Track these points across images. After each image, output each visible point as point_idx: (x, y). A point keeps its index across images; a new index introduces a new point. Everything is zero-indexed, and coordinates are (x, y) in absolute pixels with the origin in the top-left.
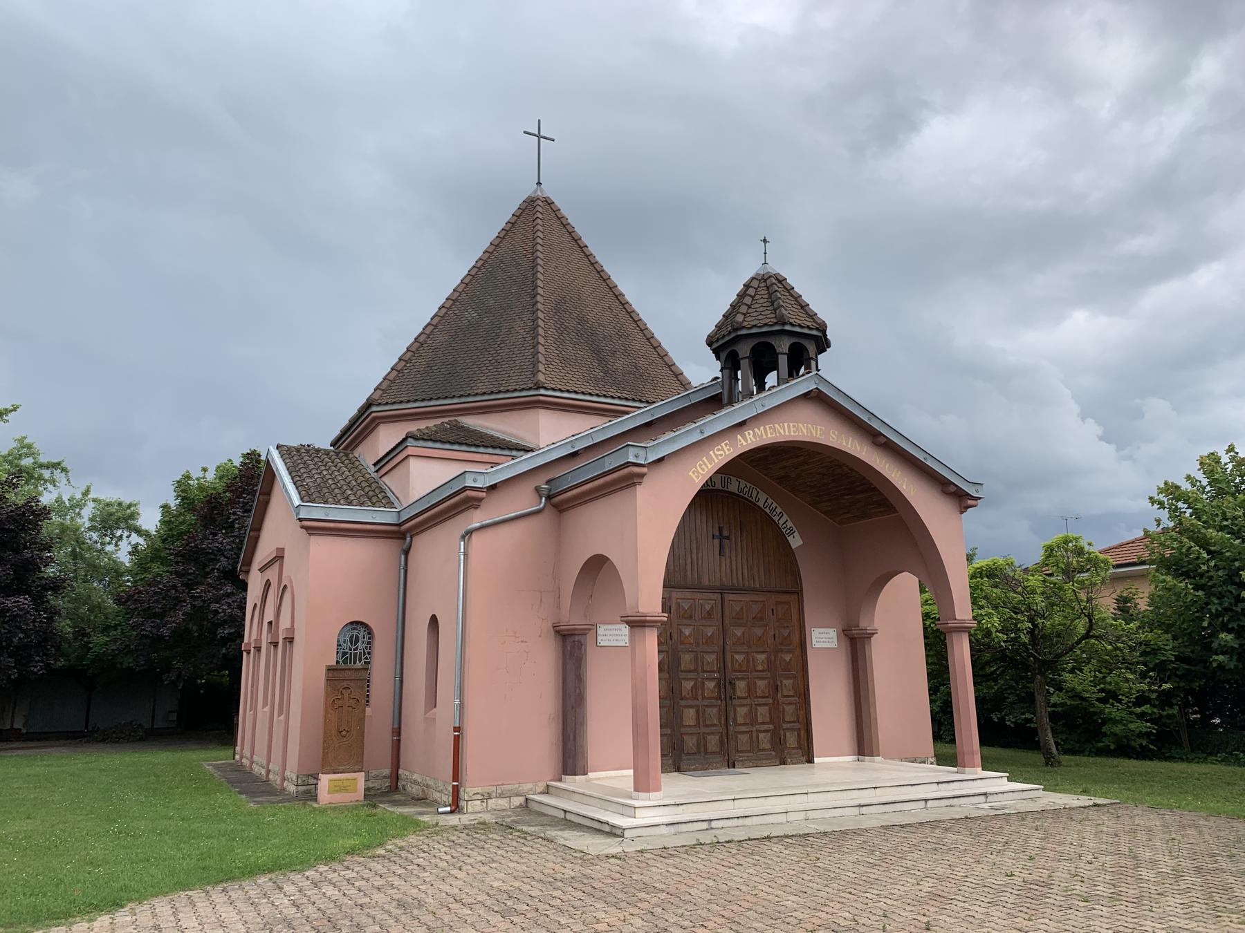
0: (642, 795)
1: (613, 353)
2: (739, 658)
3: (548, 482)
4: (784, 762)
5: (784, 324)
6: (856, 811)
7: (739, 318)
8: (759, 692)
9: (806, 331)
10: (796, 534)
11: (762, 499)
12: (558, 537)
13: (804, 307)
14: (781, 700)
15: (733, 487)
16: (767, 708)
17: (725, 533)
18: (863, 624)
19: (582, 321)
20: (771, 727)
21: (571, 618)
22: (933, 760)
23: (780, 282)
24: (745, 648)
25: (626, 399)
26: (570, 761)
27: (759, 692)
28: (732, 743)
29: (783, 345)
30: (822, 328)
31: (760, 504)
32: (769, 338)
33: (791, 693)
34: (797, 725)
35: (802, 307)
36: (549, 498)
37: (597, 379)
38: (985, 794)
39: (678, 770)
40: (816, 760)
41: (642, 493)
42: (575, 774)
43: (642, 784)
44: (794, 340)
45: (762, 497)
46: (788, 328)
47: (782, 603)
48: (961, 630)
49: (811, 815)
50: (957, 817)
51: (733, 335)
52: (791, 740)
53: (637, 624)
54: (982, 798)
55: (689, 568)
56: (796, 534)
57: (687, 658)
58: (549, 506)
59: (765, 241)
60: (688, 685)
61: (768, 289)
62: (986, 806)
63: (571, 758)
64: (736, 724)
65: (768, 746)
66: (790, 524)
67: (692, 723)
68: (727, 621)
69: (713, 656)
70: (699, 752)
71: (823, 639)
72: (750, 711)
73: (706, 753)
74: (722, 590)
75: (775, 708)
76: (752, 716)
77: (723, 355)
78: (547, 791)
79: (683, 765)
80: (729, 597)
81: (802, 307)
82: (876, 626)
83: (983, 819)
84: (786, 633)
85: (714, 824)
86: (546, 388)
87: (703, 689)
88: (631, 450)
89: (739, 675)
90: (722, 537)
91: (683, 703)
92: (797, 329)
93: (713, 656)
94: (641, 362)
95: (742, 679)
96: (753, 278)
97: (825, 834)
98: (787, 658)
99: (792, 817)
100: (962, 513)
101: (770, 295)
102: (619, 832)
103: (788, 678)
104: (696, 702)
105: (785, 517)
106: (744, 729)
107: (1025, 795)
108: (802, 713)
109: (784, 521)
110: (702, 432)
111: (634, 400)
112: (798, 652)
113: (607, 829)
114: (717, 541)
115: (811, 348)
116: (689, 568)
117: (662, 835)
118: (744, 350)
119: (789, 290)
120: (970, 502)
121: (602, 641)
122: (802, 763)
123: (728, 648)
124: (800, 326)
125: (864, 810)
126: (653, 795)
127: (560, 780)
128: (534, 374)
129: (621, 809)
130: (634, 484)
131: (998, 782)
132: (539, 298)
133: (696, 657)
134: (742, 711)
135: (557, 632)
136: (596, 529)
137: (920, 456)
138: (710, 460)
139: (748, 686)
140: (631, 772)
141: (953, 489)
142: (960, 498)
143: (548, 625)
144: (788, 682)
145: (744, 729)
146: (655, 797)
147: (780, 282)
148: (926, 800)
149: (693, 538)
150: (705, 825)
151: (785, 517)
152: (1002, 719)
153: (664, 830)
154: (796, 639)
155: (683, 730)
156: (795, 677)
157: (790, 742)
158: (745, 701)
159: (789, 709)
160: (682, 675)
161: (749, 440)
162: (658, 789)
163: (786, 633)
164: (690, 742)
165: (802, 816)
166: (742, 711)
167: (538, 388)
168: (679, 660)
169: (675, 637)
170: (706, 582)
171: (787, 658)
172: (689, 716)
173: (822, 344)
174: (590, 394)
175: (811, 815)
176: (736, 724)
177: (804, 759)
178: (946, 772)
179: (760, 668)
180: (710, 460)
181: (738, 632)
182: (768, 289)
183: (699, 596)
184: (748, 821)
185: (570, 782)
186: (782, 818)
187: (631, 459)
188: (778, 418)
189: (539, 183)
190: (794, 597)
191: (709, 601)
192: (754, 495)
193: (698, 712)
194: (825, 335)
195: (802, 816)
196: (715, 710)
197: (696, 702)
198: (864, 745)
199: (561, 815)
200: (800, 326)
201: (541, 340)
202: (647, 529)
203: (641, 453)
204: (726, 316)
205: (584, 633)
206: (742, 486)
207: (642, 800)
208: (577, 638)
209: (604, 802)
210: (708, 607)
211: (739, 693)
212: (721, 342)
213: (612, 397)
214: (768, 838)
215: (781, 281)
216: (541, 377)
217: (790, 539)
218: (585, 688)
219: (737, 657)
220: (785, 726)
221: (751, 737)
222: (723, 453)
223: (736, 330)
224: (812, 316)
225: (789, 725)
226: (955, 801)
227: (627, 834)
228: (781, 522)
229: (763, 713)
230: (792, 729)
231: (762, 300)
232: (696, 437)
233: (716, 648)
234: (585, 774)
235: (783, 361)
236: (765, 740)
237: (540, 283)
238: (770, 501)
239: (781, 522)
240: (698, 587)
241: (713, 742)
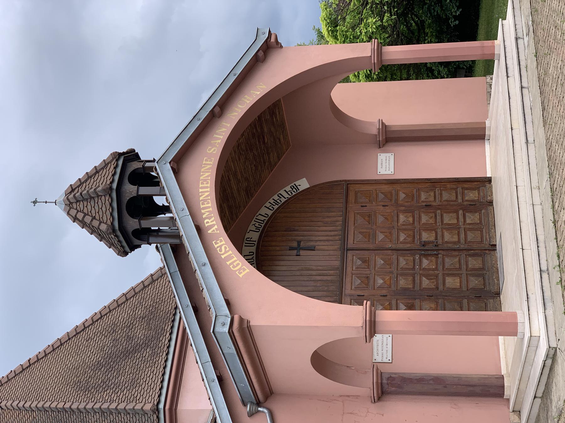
0: (520, 330)
1: (129, 338)
2: (402, 237)
3: (245, 405)
4: (491, 203)
5: (111, 188)
6: (531, 146)
7: (103, 227)
8: (432, 221)
9: (119, 170)
10: (297, 183)
11: (266, 211)
12: (296, 396)
13: (97, 171)
14: (438, 203)
15: (255, 236)
16: (445, 215)
17: (295, 244)
18: (374, 131)
19: (98, 366)
20: (461, 212)
21: (366, 386)
22: (488, 78)
23: (73, 190)
24: (395, 232)
25: (172, 327)
26: (492, 391)
27: (432, 221)
28: (475, 246)
29: (130, 190)
30: (117, 156)
31: (270, 213)
32: (125, 203)
33: (432, 194)
34: (460, 190)
35: (97, 172)
36: (259, 404)
37: (153, 354)
38: (517, 39)
39: (498, 294)
40: (489, 175)
41: (257, 320)
42: (503, 387)
43: (510, 328)
44: (126, 181)
45: (264, 211)
46: (115, 186)
47: (356, 197)
48: (380, 53)
49: (535, 184)
50: (535, 63)
51: (119, 233)
52: (472, 195)
53: (372, 328)
54: (520, 41)
55: (325, 278)
56: (297, 183)
57: (402, 283)
58: (265, 404)
59: (35, 202)
60: (426, 282)
61: (78, 202)
62: (526, 39)
63: (490, 389)
64: (459, 241)
65: (477, 215)
66: (288, 188)
67: (458, 280)
68: (371, 246)
69: (401, 259)
70: (483, 276)
71: (386, 165)
72: (448, 229)
73: (483, 269)
74: (345, 250)
75: (446, 208)
76: (451, 228)
77: (136, 242)
78: (518, 412)
79: (494, 289)
80: (351, 243)
81: (97, 172)
82: (376, 121)
83: (536, 43)
84: (381, 196)
85: (544, 268)
86: (158, 403)
87: (430, 269)
88: (217, 329)
89: (417, 237)
90: (299, 248)
91: (441, 288)
92: (117, 178)
93: (401, 259)
94: (139, 312)
95: (420, 235)
96: (68, 214)
97: (551, 174)
98: (402, 196)
99: (537, 200)
100: (281, 47)
101: (84, 200)
102: (552, 352)
103: (419, 196)
104: (440, 277)
105: (282, 192)
106: (462, 236)
107: (517, 6)
108: (448, 186)
109: (285, 193)
110: (204, 265)
111: (173, 321)
112: (397, 187)
113: (549, 362)
114: (302, 252)
115: (135, 165)
116: (325, 278)
117: (554, 313)
118: (133, 224)
119: (81, 183)
120: (273, 40)
121: (387, 358)
122: (491, 187)
123: (394, 246)
124: (114, 175)
125: (530, 139)
126: (520, 319)
127: (508, 400)
128: (145, 413)
129: (532, 349)
130: (249, 327)
131: (507, 27)
132: (74, 406)
133: (402, 275)
134: (447, 237)
135: (379, 399)
136: (288, 362)
137: (232, 79)
138: (229, 258)
139: (426, 230)
140: (501, 338)
141: (261, 54)
142: (269, 48)
143: (373, 408)
144: (423, 197)
145: (462, 236)
146: (522, 318)
147: (73, 190)
148: (522, 88)
149: (298, 273)
150: (545, 276)
151: (282, 192)
152: (456, 18)
153: (550, 312)
154: (386, 188)
155: (464, 289)
156: (419, 190)
157: (473, 197)
158: (439, 234)
159: (446, 196)
160: (417, 288)
161: (213, 223)
162: (514, 315)
163: (381, 196)
164: (474, 282)
165: (536, 192)
166: (447, 237)
167: (158, 410)
168: (405, 289)
169: (384, 292)
170: (337, 263)
171: (402, 196)
172: (452, 282)
173: (131, 156)
174: (166, 361)
175: (535, 184)
177: (488, 185)
178: (499, 68)
179: (411, 219)
180: (229, 258)
181: (381, 237)
182: (78, 202)
183: (349, 269)
184: (541, 238)
185: (510, 391)
186: (538, 209)
187: (226, 329)
188: (194, 199)
190: (352, 188)
191: (354, 261)
192: (263, 218)
193: (449, 275)
194: (124, 153)
195: (536, 192)
196: (447, 260)
197: (440, 277)
198: (476, 135)
199: (538, 401)
200: (114, 175)
201: (113, 406)
202: (290, 318)
203: (221, 320)
204: (101, 238)
205: (380, 375)
206: (254, 228)
207: (524, 329)
208: (385, 381)
209: (527, 362)
210: (359, 262)
211: (432, 239)
212: (124, 244)
213: (170, 341)
214: (555, 222)
215: (72, 189)
216: (148, 407)
217: (301, 189)
218: (429, 375)
219: (402, 238)
220: (460, 200)
221: (470, 230)
222: (224, 246)
223: (114, 231)
224: (106, 164)
225: (460, 197)
226: (523, 63)
227: (553, 345)
228: (286, 196)
229: (449, 219)
230: (463, 194)
231: (88, 207)
232: (208, 269)
233: (394, 257)
234: (502, 377)
235: (145, 191)
236: (472, 218)
237: (61, 405)
238: (268, 204)
239: (286, 196)
240: (342, 270)
241: (474, 263)
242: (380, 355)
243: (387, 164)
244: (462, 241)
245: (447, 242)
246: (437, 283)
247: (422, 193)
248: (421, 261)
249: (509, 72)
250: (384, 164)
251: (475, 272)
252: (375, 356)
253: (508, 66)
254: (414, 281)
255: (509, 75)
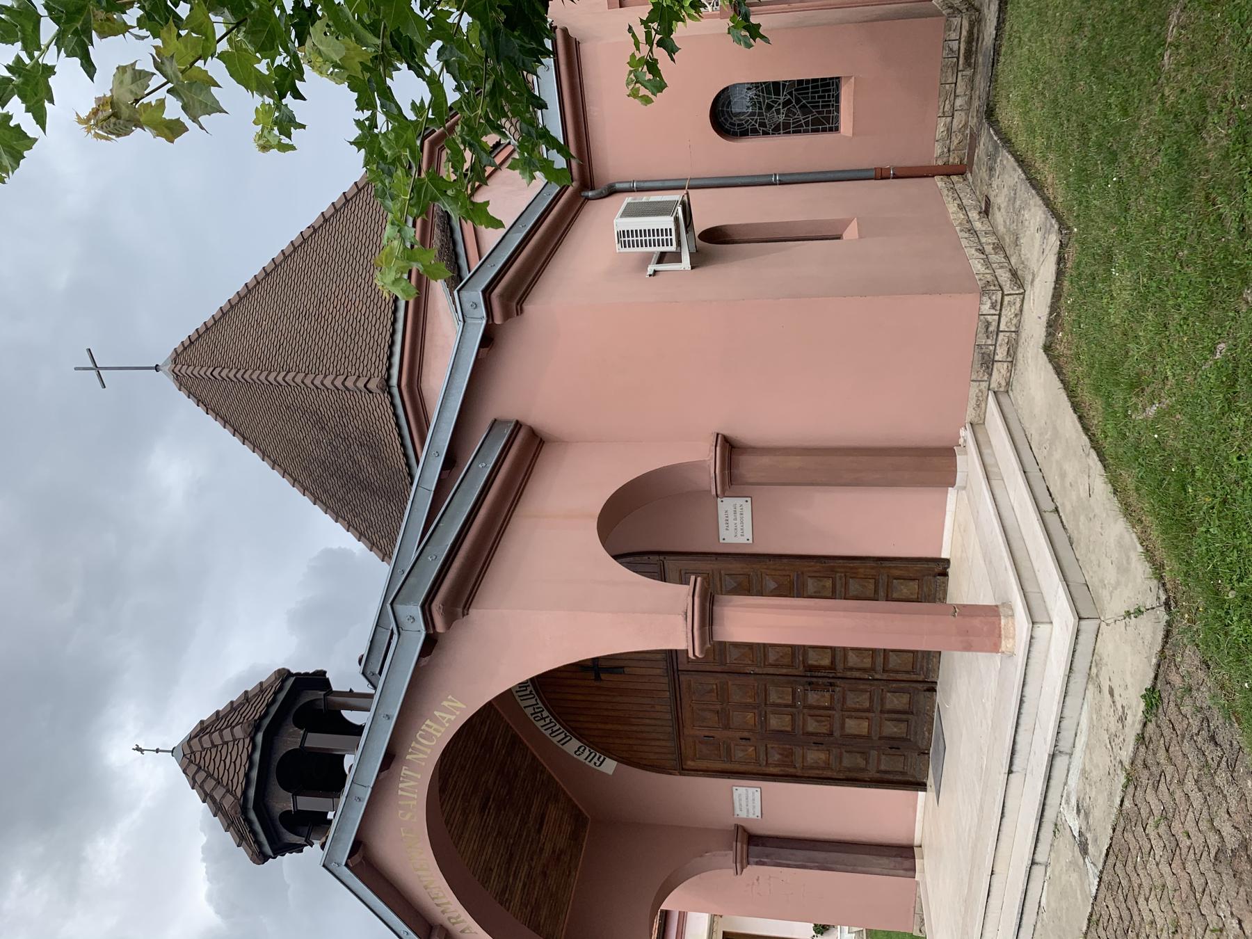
38: (1053, 757)
40: (944, 555)
57: (774, 722)
64: (873, 669)
68: (719, 669)
91: (837, 734)
122: (945, 584)
148: (1033, 863)
164: (891, 729)
172: (855, 726)
176: (873, 669)
189: (157, 368)
196: (850, 695)
241: (896, 701)
242: (745, 811)
243: (738, 521)
244: (879, 668)
245: (851, 669)
246: (831, 725)
247: (810, 581)
248: (805, 695)
249: (1017, 761)
250: (731, 522)
251: (895, 716)
252: (737, 811)
253: (1018, 747)
254: (793, 720)
255: (1015, 768)
